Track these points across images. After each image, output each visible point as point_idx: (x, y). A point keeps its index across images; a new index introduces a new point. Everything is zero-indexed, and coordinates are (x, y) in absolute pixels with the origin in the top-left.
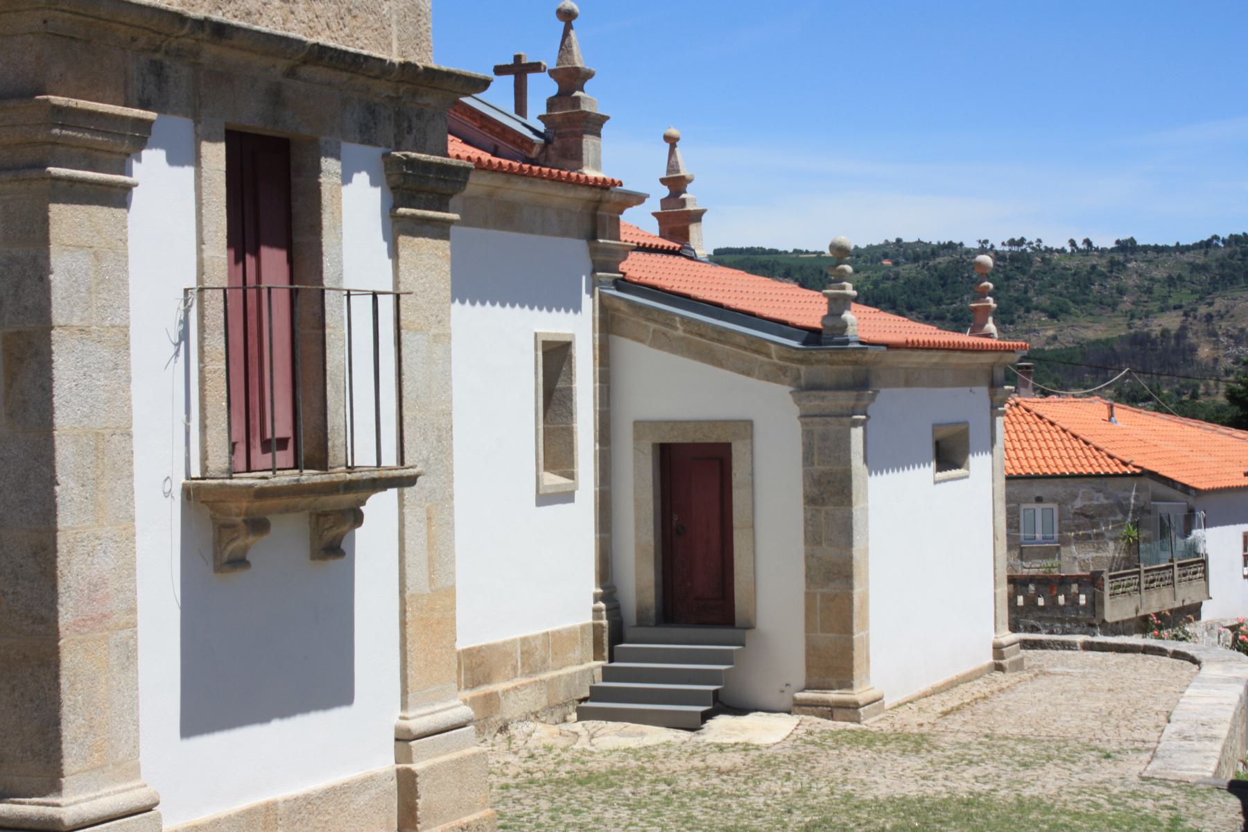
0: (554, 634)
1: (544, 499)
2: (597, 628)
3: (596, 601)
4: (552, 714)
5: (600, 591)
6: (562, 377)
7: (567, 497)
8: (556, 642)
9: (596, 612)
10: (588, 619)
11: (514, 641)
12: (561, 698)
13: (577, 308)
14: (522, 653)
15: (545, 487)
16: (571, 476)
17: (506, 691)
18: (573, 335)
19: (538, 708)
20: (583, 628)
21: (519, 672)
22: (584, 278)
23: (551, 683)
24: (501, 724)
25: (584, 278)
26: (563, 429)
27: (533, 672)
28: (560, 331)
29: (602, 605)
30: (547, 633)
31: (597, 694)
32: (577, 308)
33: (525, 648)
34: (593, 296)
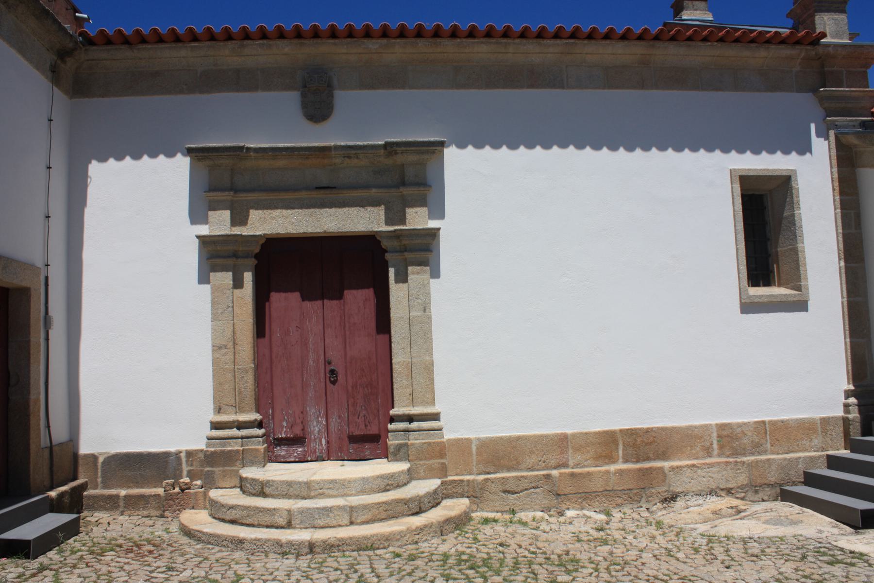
0: (773, 423)
1: (748, 307)
2: (846, 421)
3: (847, 398)
4: (756, 492)
5: (852, 387)
6: (787, 207)
7: (801, 306)
8: (806, 428)
9: (846, 406)
10: (840, 413)
11: (706, 427)
12: (773, 480)
13: (804, 148)
14: (719, 436)
15: (750, 297)
16: (798, 288)
17: (672, 469)
18: (795, 171)
19: (730, 486)
20: (825, 421)
21: (716, 452)
22: (813, 126)
23: (751, 466)
24: (666, 495)
25: (813, 126)
26: (791, 250)
27: (735, 454)
28: (771, 167)
29: (852, 400)
30: (764, 422)
31: (811, 480)
32: (804, 148)
33: (725, 433)
34: (827, 138)
